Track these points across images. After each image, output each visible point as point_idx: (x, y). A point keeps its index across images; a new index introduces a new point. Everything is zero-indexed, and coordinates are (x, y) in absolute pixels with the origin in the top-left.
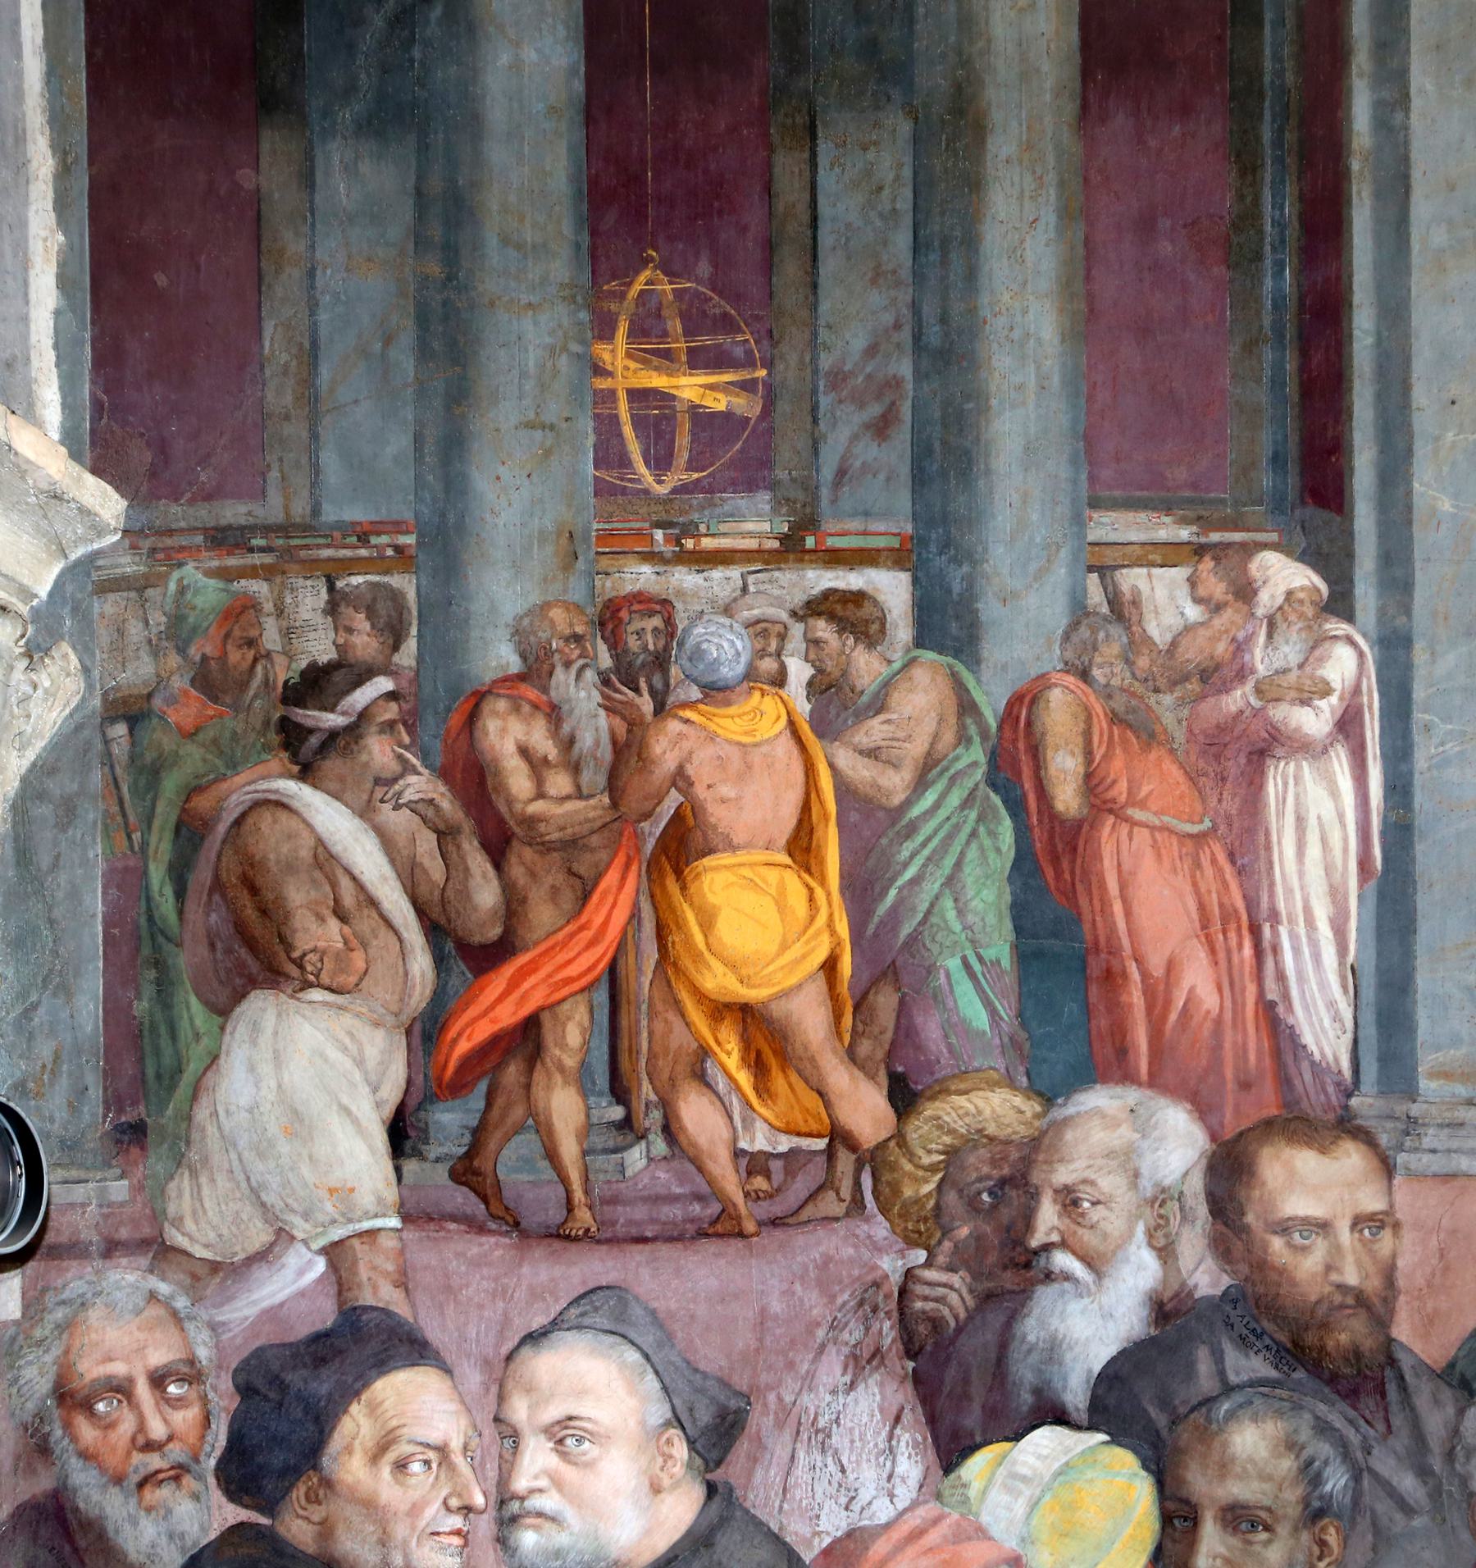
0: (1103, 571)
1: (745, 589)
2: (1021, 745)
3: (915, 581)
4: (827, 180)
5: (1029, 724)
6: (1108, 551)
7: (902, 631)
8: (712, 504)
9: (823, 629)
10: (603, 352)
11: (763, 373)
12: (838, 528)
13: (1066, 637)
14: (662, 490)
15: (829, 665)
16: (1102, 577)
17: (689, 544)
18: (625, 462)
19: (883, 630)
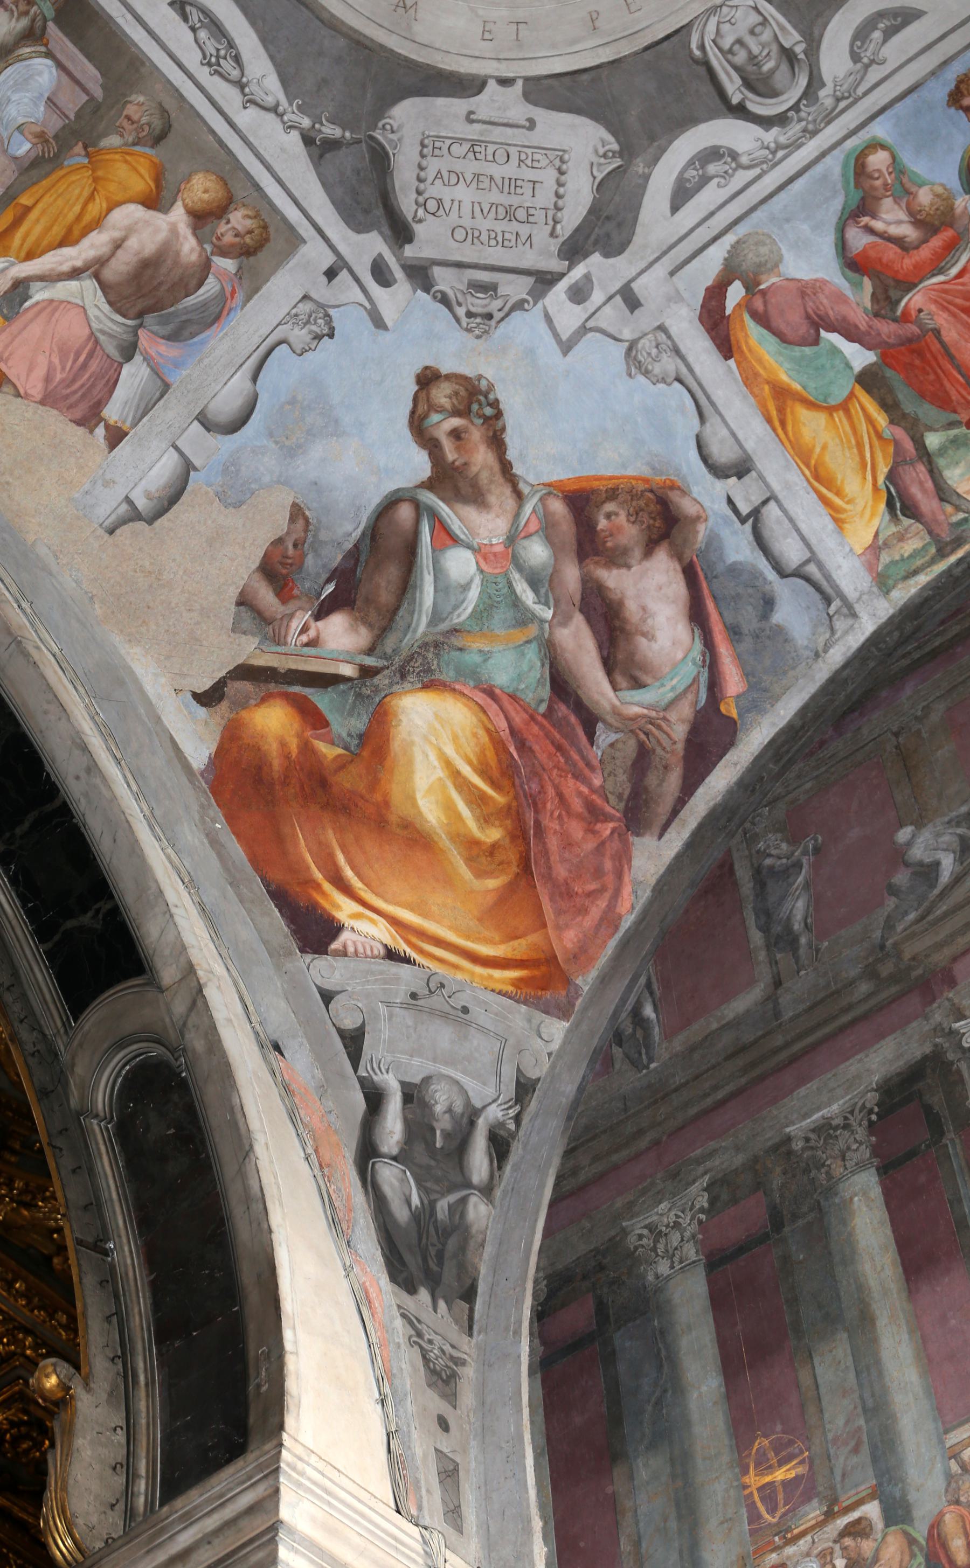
0: (955, 1457)
1: (813, 1542)
2: (938, 1546)
3: (881, 1502)
4: (819, 1370)
5: (939, 1535)
6: (956, 1448)
7: (879, 1524)
8: (795, 1515)
9: (848, 1541)
10: (746, 1480)
11: (807, 1453)
12: (846, 1496)
13: (947, 1491)
14: (775, 1520)
15: (853, 1555)
16: (956, 1460)
17: (789, 1536)
18: (760, 1517)
19: (871, 1529)
